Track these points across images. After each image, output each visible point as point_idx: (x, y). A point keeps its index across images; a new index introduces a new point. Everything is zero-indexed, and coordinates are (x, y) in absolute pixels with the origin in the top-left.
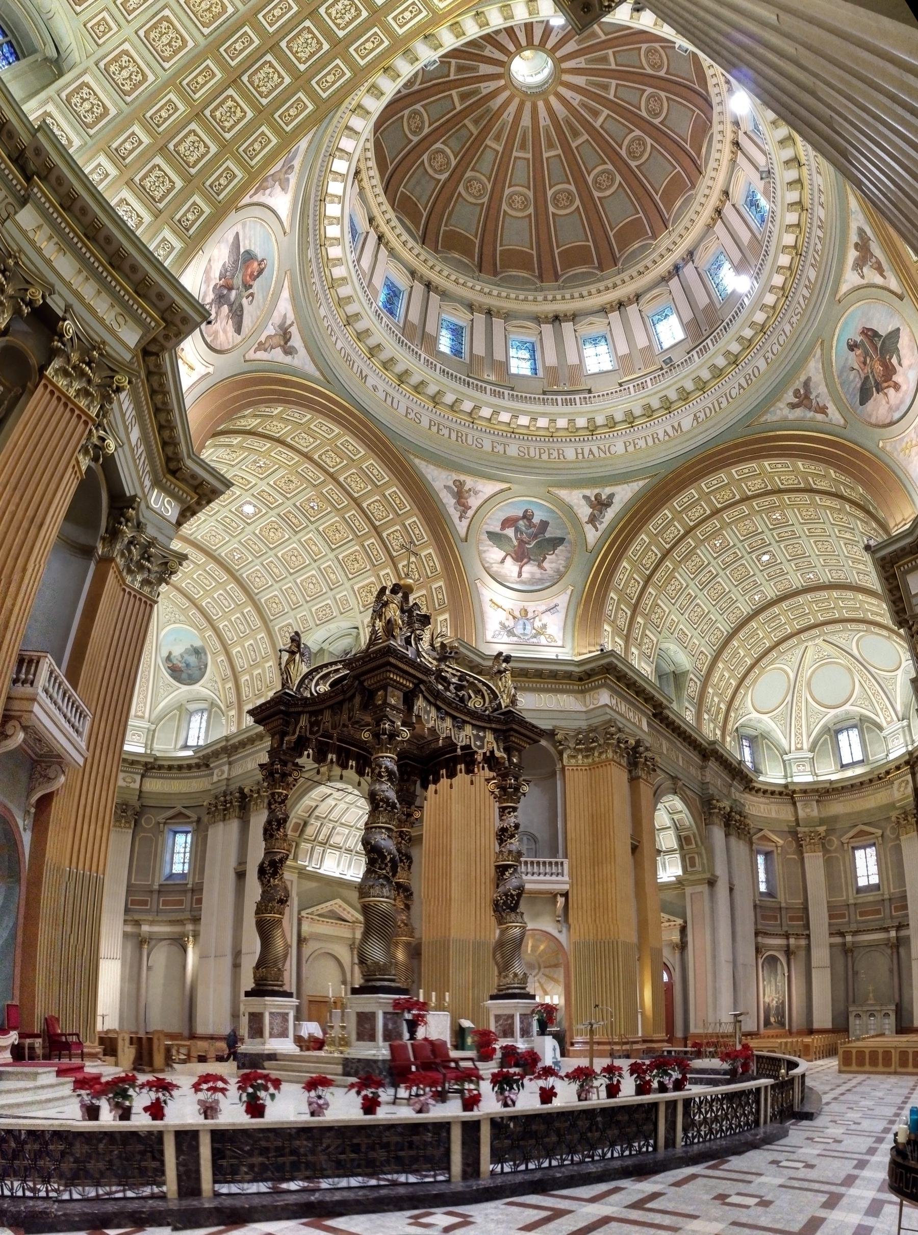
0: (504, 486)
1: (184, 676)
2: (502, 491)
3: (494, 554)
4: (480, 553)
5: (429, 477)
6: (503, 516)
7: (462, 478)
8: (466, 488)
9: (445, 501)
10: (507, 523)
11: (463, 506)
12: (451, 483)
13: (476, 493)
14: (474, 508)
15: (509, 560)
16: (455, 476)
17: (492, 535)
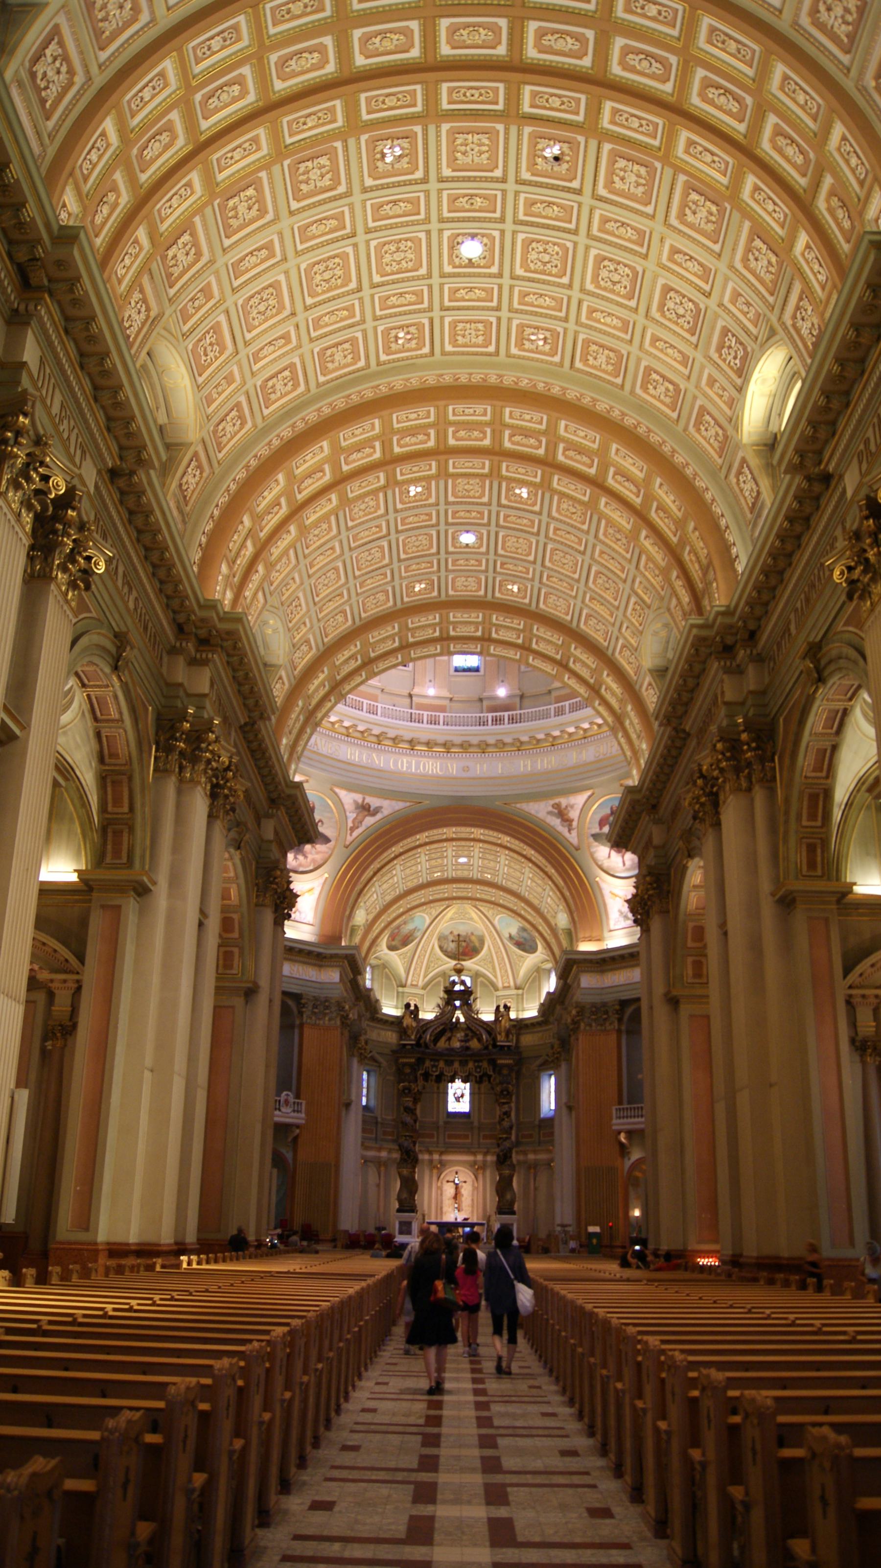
0: (589, 793)
1: (527, 948)
2: (590, 797)
3: (603, 851)
4: (592, 855)
5: (533, 812)
6: (598, 817)
7: (557, 801)
8: (563, 805)
9: (552, 824)
10: (602, 823)
11: (567, 821)
12: (550, 809)
13: (572, 807)
14: (576, 819)
15: (613, 853)
16: (552, 802)
17: (596, 837)
